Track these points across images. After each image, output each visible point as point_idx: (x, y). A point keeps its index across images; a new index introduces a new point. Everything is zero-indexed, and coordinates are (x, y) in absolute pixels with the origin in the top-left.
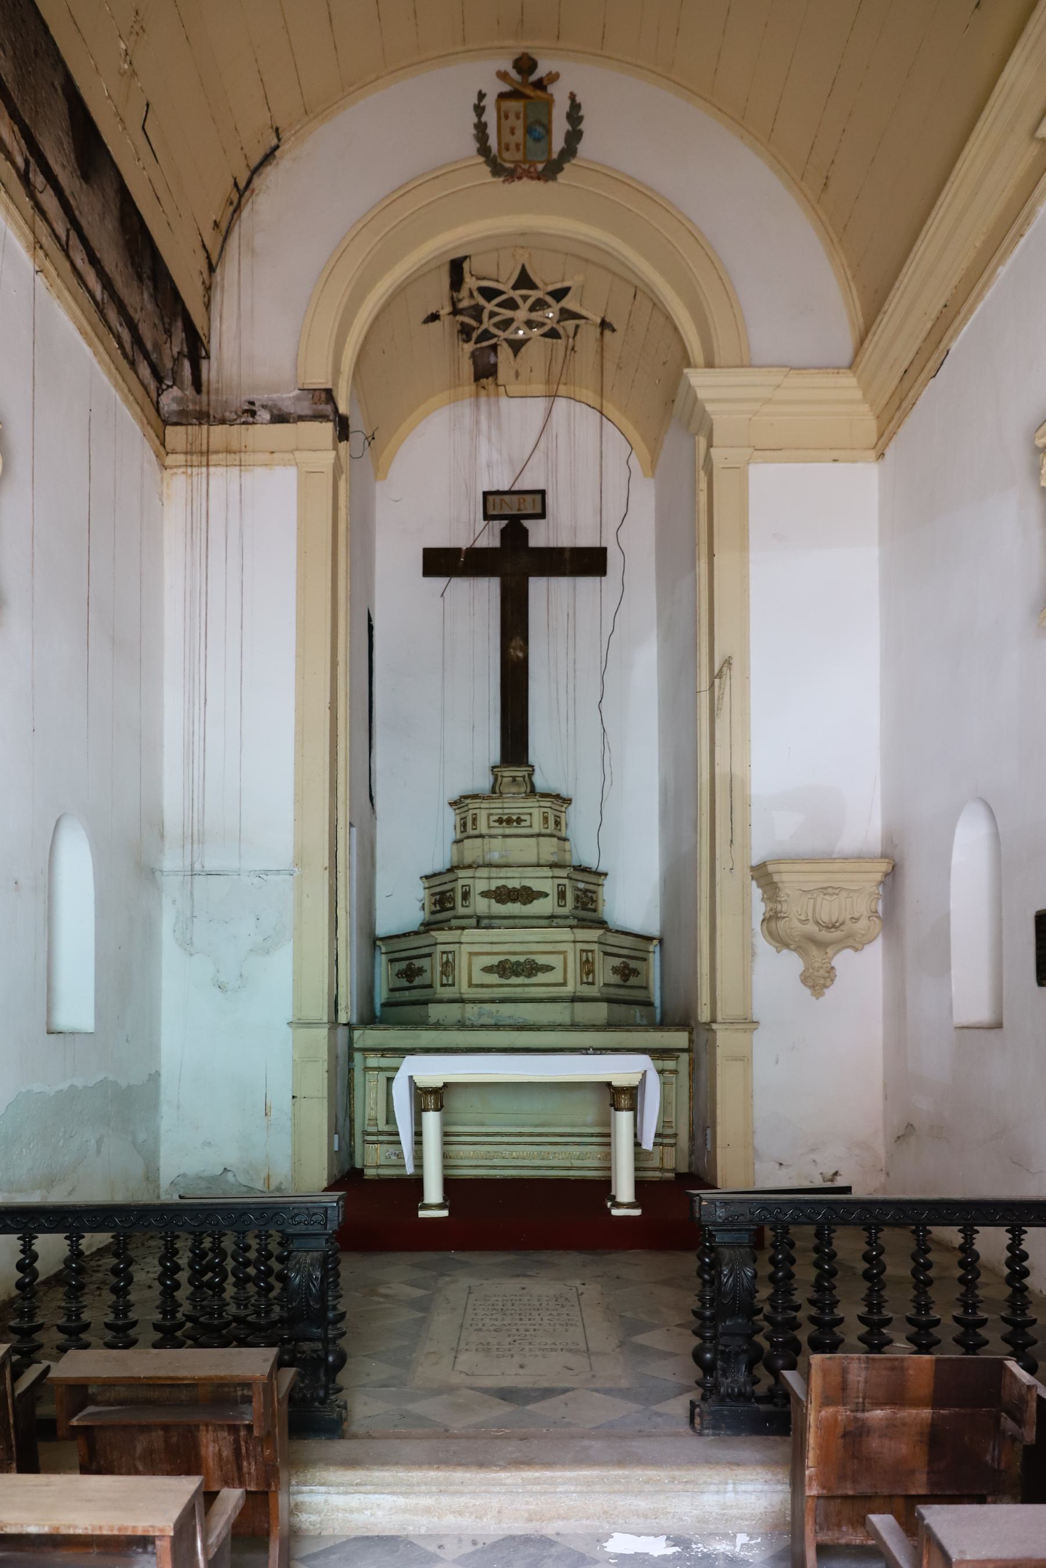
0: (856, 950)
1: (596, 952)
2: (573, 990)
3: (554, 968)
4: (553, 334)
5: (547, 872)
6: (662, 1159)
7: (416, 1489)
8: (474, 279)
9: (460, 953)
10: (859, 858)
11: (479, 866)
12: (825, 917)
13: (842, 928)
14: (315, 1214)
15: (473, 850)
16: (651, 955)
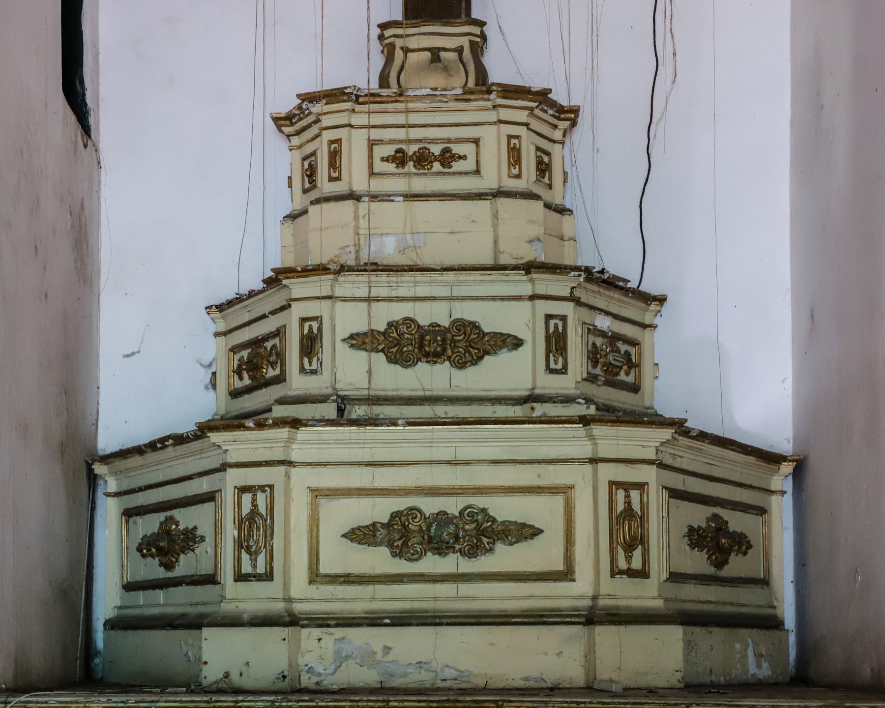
2: (590, 592)
3: (540, 531)
5: (521, 285)
11: (343, 269)
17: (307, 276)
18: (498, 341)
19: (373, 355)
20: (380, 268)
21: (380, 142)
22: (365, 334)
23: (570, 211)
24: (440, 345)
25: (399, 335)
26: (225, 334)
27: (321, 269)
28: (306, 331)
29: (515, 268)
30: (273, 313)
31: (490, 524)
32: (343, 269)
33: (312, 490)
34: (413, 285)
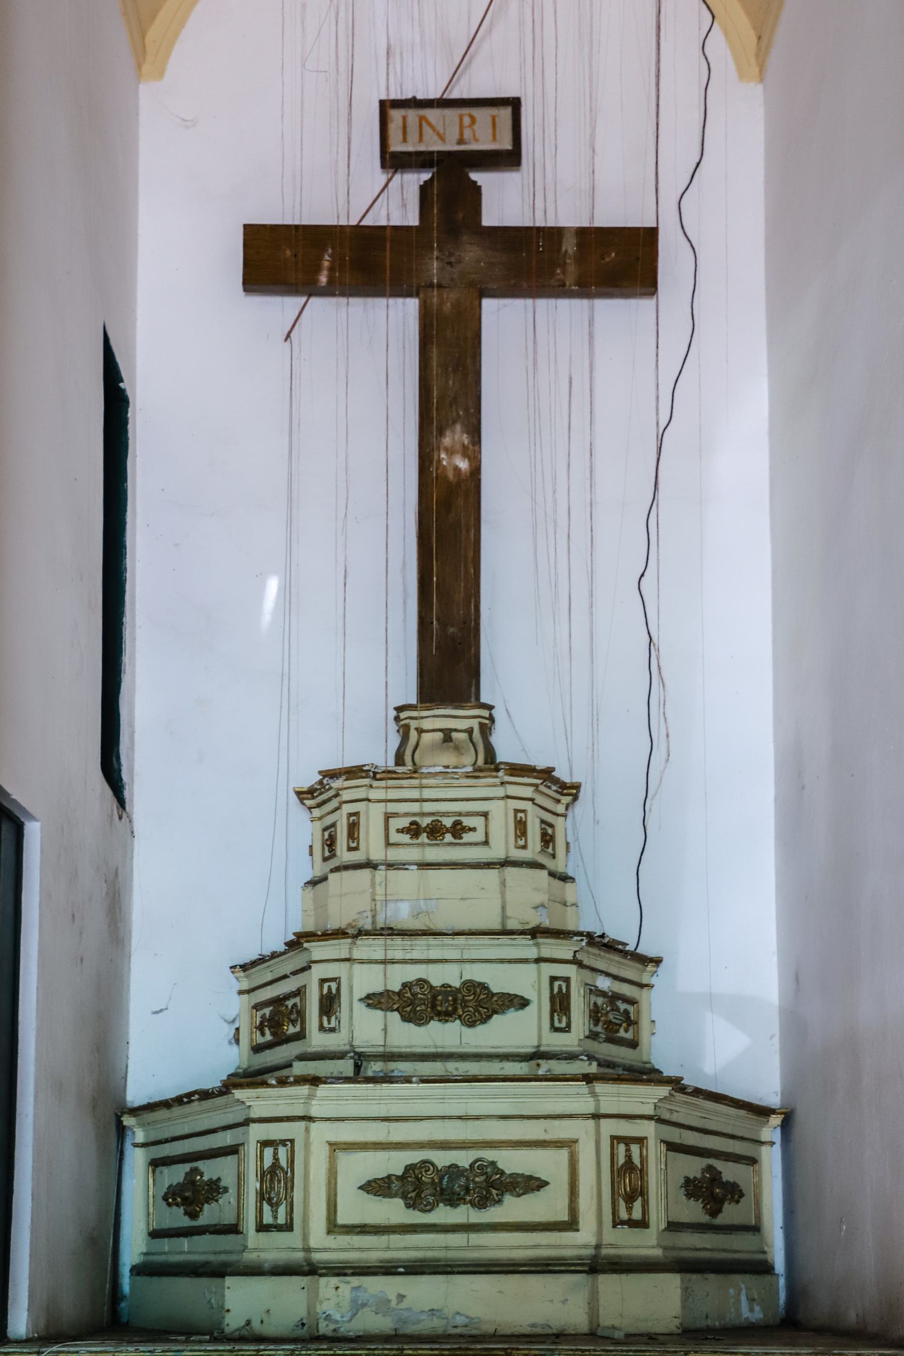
2: (593, 1241)
3: (546, 1183)
5: (526, 948)
9: (307, 1145)
11: (361, 933)
16: (764, 1149)
17: (327, 940)
18: (506, 1001)
19: (389, 1014)
20: (396, 932)
21: (396, 815)
22: (381, 994)
23: (572, 879)
24: (451, 1005)
25: (412, 995)
26: (249, 992)
27: (339, 934)
28: (325, 991)
29: (522, 933)
30: (294, 973)
31: (498, 1176)
32: (361, 933)
33: (331, 1144)
34: (427, 948)
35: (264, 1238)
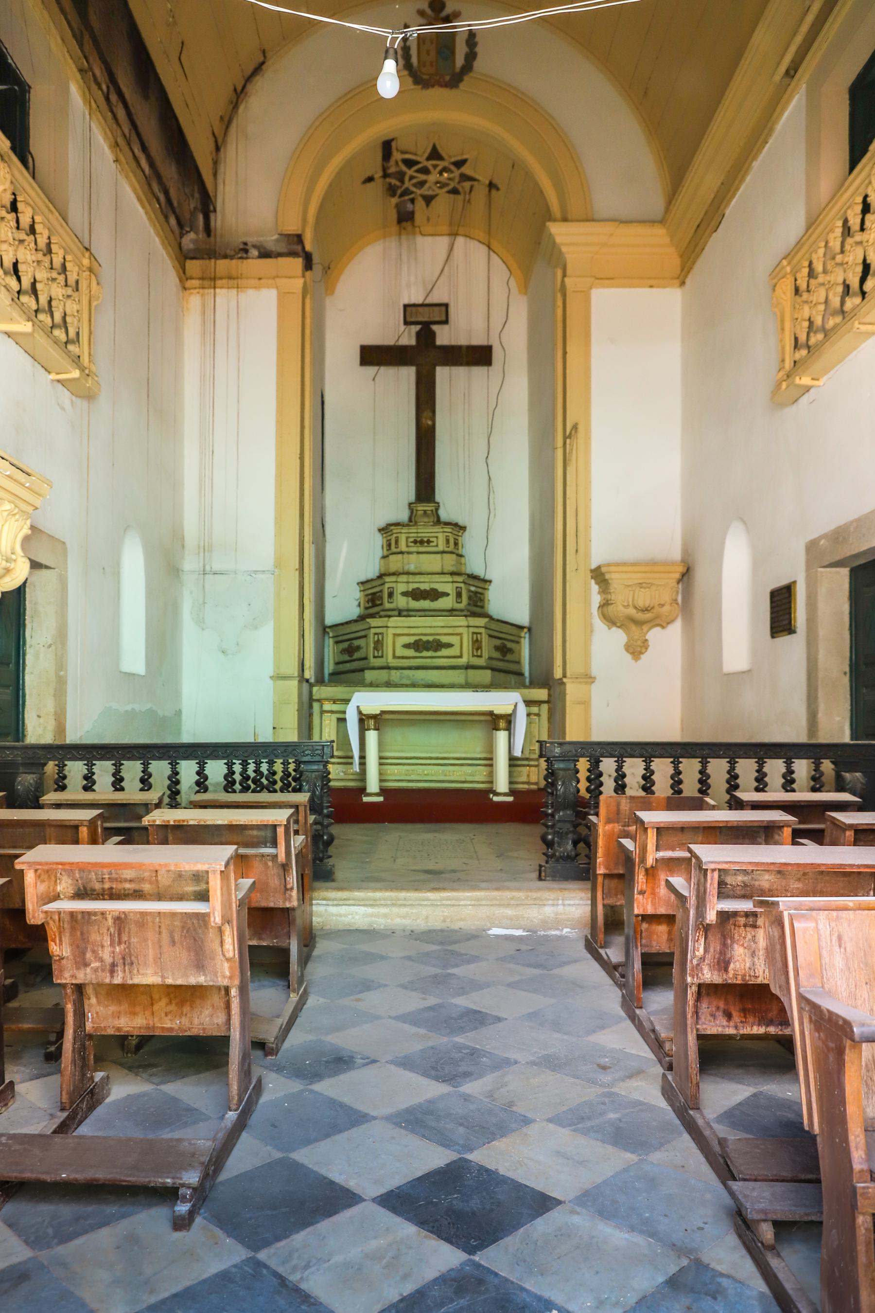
0: (663, 627)
1: (484, 635)
2: (467, 661)
4: (455, 191)
5: (449, 578)
6: (528, 776)
7: (378, 903)
8: (399, 153)
9: (387, 635)
10: (665, 563)
11: (400, 574)
12: (641, 603)
13: (652, 611)
14: (317, 750)
15: (395, 563)
27: (394, 574)
30: (379, 585)
35: (375, 660)
